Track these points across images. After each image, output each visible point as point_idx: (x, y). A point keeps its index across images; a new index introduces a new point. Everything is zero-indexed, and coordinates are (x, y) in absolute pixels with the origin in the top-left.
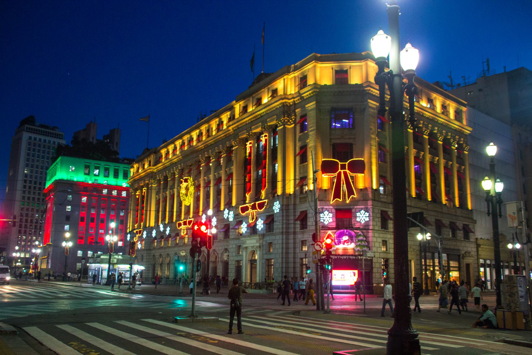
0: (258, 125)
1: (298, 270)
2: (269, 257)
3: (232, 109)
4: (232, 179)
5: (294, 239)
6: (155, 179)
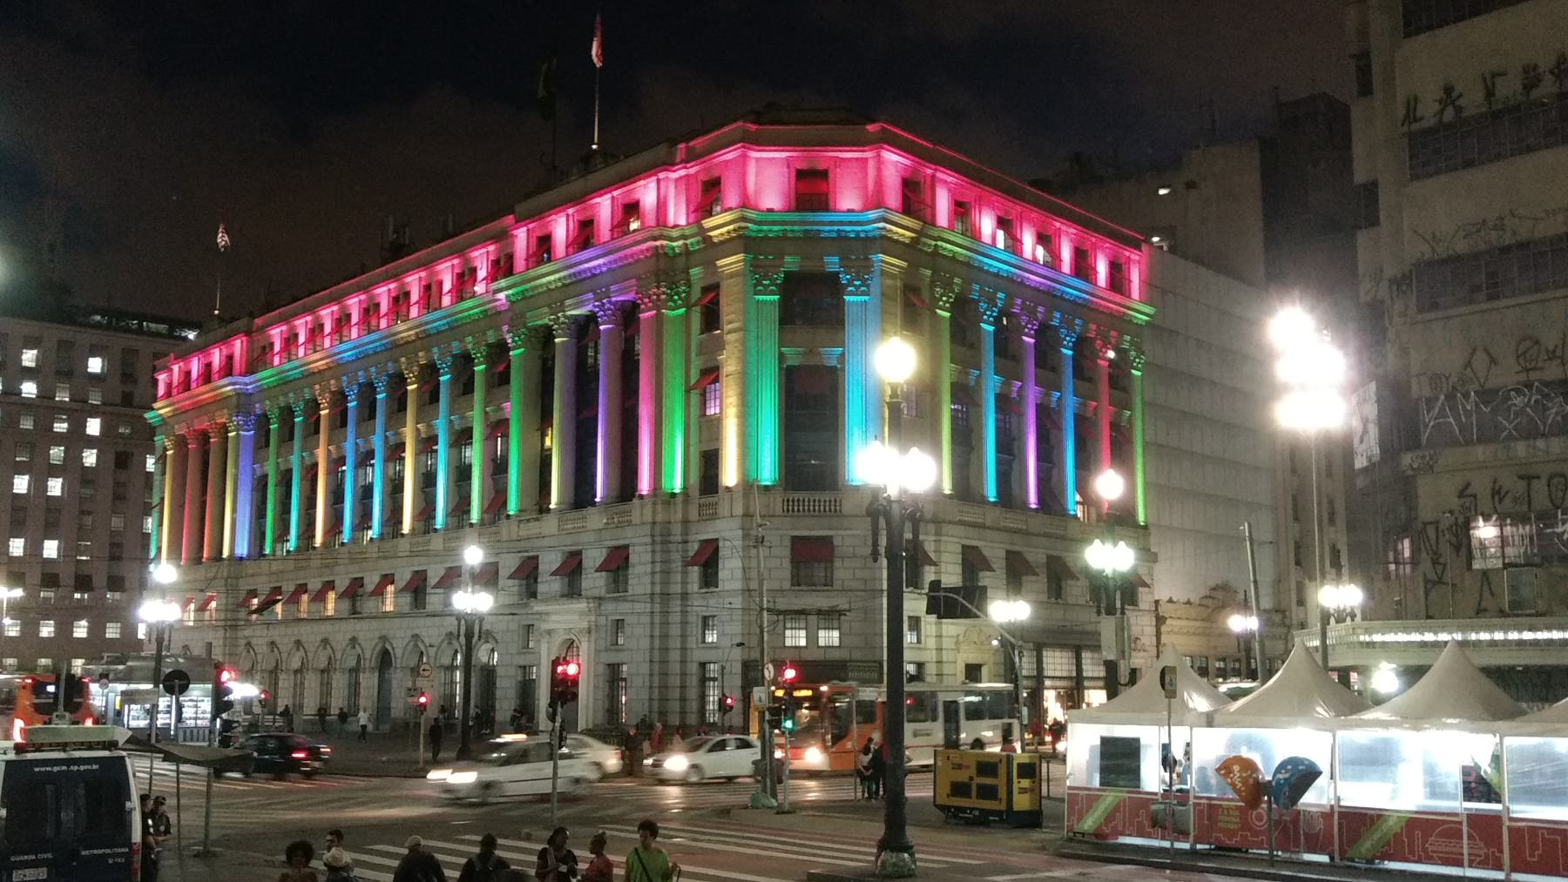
0: (585, 297)
1: (693, 693)
2: (613, 658)
3: (503, 237)
4: (506, 436)
5: (684, 613)
6: (248, 414)
